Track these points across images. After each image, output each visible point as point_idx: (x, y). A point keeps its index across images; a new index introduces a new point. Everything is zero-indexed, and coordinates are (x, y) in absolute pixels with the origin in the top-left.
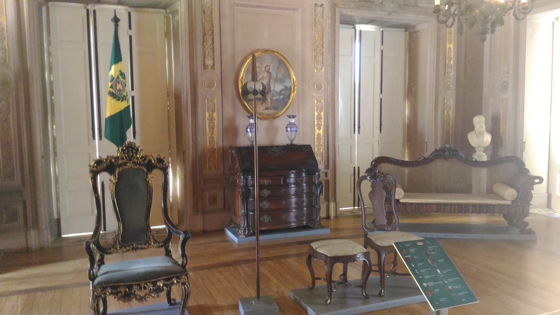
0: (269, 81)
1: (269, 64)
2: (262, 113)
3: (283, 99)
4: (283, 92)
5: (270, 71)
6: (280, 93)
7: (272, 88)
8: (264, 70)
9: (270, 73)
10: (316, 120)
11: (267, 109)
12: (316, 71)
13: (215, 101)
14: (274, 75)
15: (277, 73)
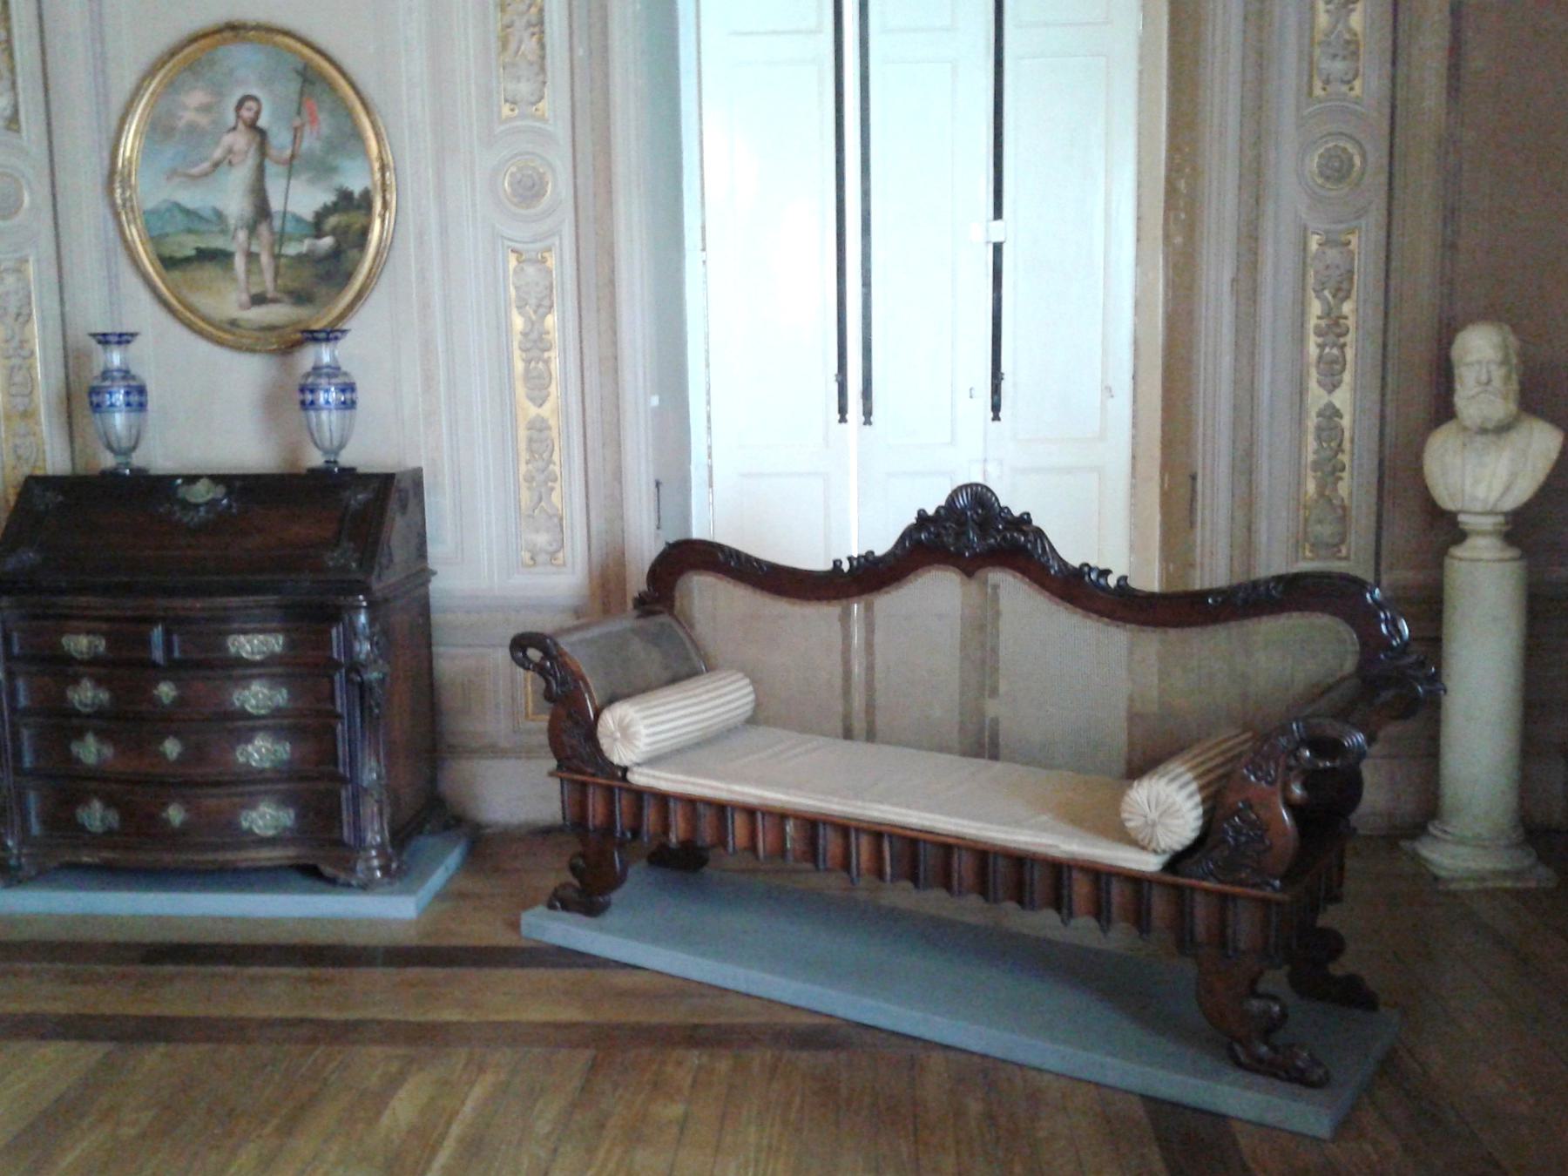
0: (260, 171)
1: (255, 92)
2: (234, 323)
3: (336, 254)
4: (333, 221)
5: (262, 122)
6: (317, 227)
7: (276, 204)
8: (231, 118)
9: (262, 133)
10: (517, 354)
11: (259, 300)
12: (506, 110)
13: (31, 269)
14: (280, 140)
15: (297, 133)
